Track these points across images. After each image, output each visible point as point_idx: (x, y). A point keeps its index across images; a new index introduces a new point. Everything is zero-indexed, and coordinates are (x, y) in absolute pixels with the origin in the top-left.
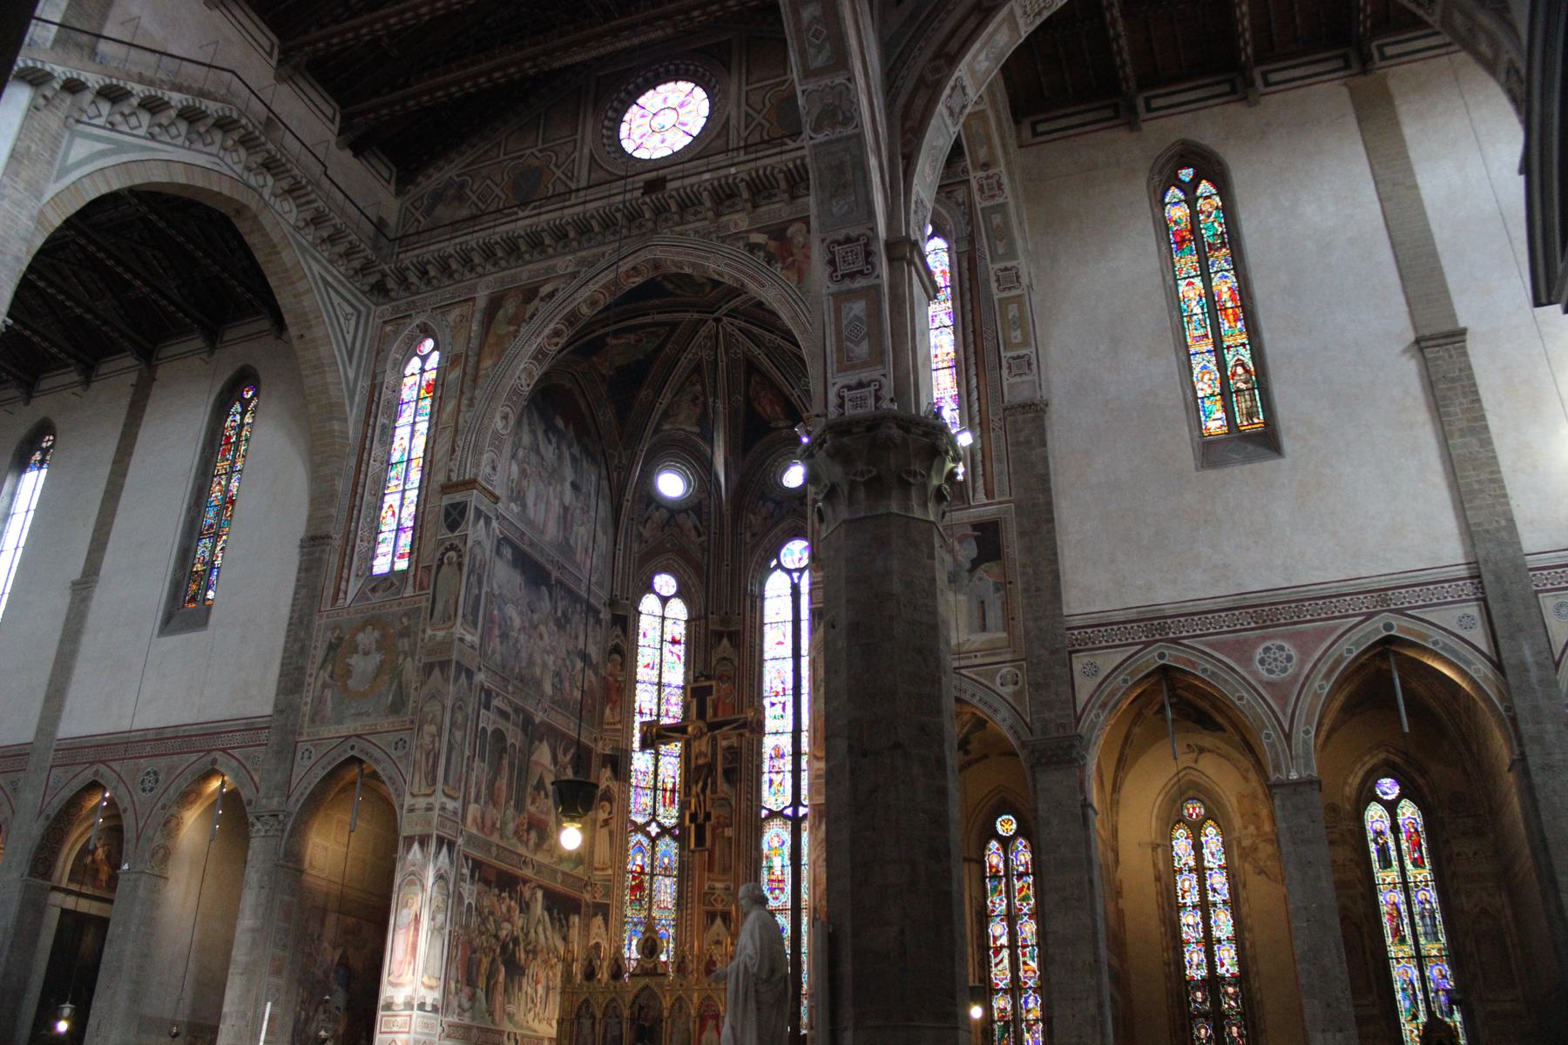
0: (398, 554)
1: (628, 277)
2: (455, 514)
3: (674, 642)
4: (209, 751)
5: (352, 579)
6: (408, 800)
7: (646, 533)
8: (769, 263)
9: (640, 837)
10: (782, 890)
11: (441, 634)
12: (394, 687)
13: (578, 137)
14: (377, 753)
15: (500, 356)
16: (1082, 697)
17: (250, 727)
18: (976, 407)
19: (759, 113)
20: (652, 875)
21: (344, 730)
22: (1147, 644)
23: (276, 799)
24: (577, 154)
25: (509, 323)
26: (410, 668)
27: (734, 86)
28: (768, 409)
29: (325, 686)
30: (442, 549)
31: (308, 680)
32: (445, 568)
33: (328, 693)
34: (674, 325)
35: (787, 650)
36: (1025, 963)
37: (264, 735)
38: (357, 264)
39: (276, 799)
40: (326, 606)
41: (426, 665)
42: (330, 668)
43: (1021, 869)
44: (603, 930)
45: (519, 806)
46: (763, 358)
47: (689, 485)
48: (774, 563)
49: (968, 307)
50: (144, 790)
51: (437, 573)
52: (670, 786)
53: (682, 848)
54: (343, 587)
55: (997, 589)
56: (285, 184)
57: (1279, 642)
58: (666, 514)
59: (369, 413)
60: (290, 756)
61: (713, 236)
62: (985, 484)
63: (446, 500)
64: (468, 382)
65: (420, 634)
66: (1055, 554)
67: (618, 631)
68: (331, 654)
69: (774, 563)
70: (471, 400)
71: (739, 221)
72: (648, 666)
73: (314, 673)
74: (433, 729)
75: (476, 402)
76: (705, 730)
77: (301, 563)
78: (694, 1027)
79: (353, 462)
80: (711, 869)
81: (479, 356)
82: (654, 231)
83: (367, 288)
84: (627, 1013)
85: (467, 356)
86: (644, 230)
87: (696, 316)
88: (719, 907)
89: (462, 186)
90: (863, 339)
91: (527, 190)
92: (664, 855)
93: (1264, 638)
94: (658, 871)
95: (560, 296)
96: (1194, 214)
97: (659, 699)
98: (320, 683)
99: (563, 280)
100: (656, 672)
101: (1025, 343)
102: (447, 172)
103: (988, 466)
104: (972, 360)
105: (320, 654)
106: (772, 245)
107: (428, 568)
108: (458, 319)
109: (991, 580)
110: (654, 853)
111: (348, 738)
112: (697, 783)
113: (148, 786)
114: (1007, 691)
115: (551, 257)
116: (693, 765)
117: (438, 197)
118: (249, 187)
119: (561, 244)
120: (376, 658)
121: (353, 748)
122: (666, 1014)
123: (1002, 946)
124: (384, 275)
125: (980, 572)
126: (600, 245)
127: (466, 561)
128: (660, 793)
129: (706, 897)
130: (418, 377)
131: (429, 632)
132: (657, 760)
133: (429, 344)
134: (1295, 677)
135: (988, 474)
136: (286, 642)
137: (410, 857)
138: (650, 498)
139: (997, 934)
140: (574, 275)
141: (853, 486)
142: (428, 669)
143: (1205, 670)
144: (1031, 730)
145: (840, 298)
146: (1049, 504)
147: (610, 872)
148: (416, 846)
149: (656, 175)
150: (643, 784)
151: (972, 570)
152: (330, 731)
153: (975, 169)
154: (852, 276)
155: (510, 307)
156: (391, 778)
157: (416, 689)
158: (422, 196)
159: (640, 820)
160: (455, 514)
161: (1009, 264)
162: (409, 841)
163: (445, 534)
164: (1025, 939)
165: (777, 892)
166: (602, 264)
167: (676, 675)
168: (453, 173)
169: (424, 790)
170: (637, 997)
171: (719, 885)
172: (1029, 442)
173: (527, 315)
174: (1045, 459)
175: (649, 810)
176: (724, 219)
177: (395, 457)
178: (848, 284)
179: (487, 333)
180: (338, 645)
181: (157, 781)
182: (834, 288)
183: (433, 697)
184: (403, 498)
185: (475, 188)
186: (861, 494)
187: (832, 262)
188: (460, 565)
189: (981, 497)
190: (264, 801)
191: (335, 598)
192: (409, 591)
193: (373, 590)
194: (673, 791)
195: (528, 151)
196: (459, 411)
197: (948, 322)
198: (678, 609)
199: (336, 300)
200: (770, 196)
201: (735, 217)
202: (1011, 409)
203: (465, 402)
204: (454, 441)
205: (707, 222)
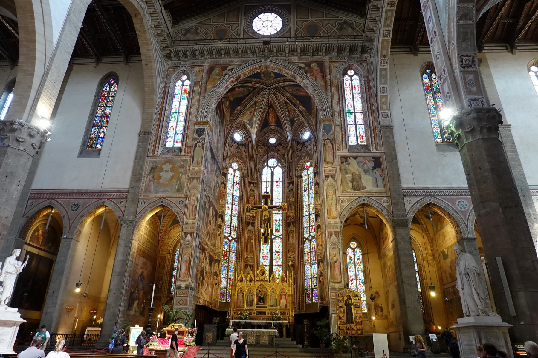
0: (175, 141)
1: (257, 69)
2: (201, 132)
3: (237, 183)
4: (101, 199)
5: (160, 147)
6: (185, 220)
7: (232, 150)
8: (306, 73)
9: (226, 240)
10: (267, 259)
11: (196, 168)
12: (178, 183)
13: (239, 22)
14: (172, 204)
15: (214, 85)
16: (407, 209)
17: (119, 192)
18: (372, 125)
19: (301, 28)
20: (229, 252)
21: (158, 196)
22: (426, 197)
23: (131, 217)
24: (239, 28)
25: (217, 75)
26: (184, 178)
27: (292, 18)
28: (271, 119)
29: (150, 181)
30: (196, 142)
31: (143, 178)
32: (197, 148)
33: (152, 183)
34: (255, 88)
36: (360, 284)
37: (125, 195)
38: (164, 45)
39: (131, 217)
40: (150, 154)
41: (191, 178)
42: (152, 175)
43: (358, 257)
44: (218, 268)
45: (207, 228)
46: (277, 104)
47: (243, 138)
48: (266, 164)
49: (368, 96)
50: (72, 210)
51: (194, 149)
52: (235, 226)
53: (238, 244)
54: (157, 149)
55: (381, 176)
56: (152, 11)
57: (463, 200)
58: (237, 145)
59: (164, 95)
60: (137, 203)
61: (287, 62)
62: (375, 146)
63: (197, 127)
64: (203, 91)
65: (188, 168)
66: (398, 169)
67: (224, 177)
68: (153, 170)
69: (266, 164)
70: (204, 97)
71: (296, 59)
72: (229, 189)
73: (146, 176)
74: (195, 198)
75: (206, 98)
76: (267, 208)
77: (139, 140)
78: (278, 298)
79: (159, 110)
80: (247, 252)
81: (206, 83)
82: (267, 57)
83: (165, 55)
84: (255, 293)
85: (202, 83)
86: (263, 56)
87: (264, 87)
88: (249, 263)
89: (197, 29)
90: (474, 86)
91: (221, 35)
92: (233, 246)
93: (459, 199)
94: (231, 251)
95: (235, 70)
96: (431, 82)
97: (233, 199)
98: (148, 179)
99: (236, 66)
100: (232, 191)
101: (387, 109)
103: (376, 141)
104: (370, 111)
105: (148, 171)
106: (307, 68)
107: (190, 147)
108: (198, 71)
109: (379, 173)
110: (230, 246)
111: (160, 198)
112: (264, 224)
113: (74, 209)
114: (385, 205)
115: (231, 58)
116: (263, 219)
117: (188, 31)
118: (141, 7)
119: (235, 54)
120: (171, 174)
121: (162, 202)
122: (268, 293)
123: (353, 279)
124: (171, 51)
125: (375, 170)
126: (248, 57)
127: (205, 147)
128: (232, 227)
129: (246, 259)
130: (181, 87)
131: (192, 167)
132: (232, 218)
134: (468, 210)
135: (376, 143)
136: (134, 165)
137: (187, 238)
138: (233, 140)
139: (352, 275)
140: (240, 65)
141: (482, 128)
142: (193, 179)
143: (442, 205)
144: (393, 216)
145: (464, 74)
146: (396, 155)
147: (220, 250)
148: (189, 235)
149: (267, 41)
150: (228, 224)
151: (373, 170)
152: (153, 196)
153: (381, 56)
154: (468, 67)
155: (217, 70)
156: (177, 213)
157: (187, 185)
158: (182, 30)
159: (227, 235)
160: (201, 132)
161: (385, 86)
162: (186, 234)
163: (196, 137)
164: (360, 277)
165: (265, 260)
166: (249, 63)
167: (237, 193)
168: (193, 24)
169: (191, 218)
170: (258, 287)
171: (249, 257)
172: (388, 137)
173: (224, 73)
174: (394, 142)
175: (229, 232)
176: (291, 57)
178: (466, 69)
179: (209, 77)
180: (156, 168)
181: (78, 207)
182: (463, 69)
183: (194, 188)
184: (177, 124)
185: (202, 31)
186: (485, 131)
187: (462, 62)
188: (203, 148)
189: (374, 150)
190: (126, 217)
191: (154, 153)
192: (183, 153)
193: (167, 152)
194: (235, 227)
195: (221, 23)
196: (200, 100)
197: (360, 100)
198: (238, 174)
199: (158, 55)
200: (305, 54)
201: (294, 57)
202: (383, 127)
203: (202, 97)
204: (198, 109)
205: (285, 57)
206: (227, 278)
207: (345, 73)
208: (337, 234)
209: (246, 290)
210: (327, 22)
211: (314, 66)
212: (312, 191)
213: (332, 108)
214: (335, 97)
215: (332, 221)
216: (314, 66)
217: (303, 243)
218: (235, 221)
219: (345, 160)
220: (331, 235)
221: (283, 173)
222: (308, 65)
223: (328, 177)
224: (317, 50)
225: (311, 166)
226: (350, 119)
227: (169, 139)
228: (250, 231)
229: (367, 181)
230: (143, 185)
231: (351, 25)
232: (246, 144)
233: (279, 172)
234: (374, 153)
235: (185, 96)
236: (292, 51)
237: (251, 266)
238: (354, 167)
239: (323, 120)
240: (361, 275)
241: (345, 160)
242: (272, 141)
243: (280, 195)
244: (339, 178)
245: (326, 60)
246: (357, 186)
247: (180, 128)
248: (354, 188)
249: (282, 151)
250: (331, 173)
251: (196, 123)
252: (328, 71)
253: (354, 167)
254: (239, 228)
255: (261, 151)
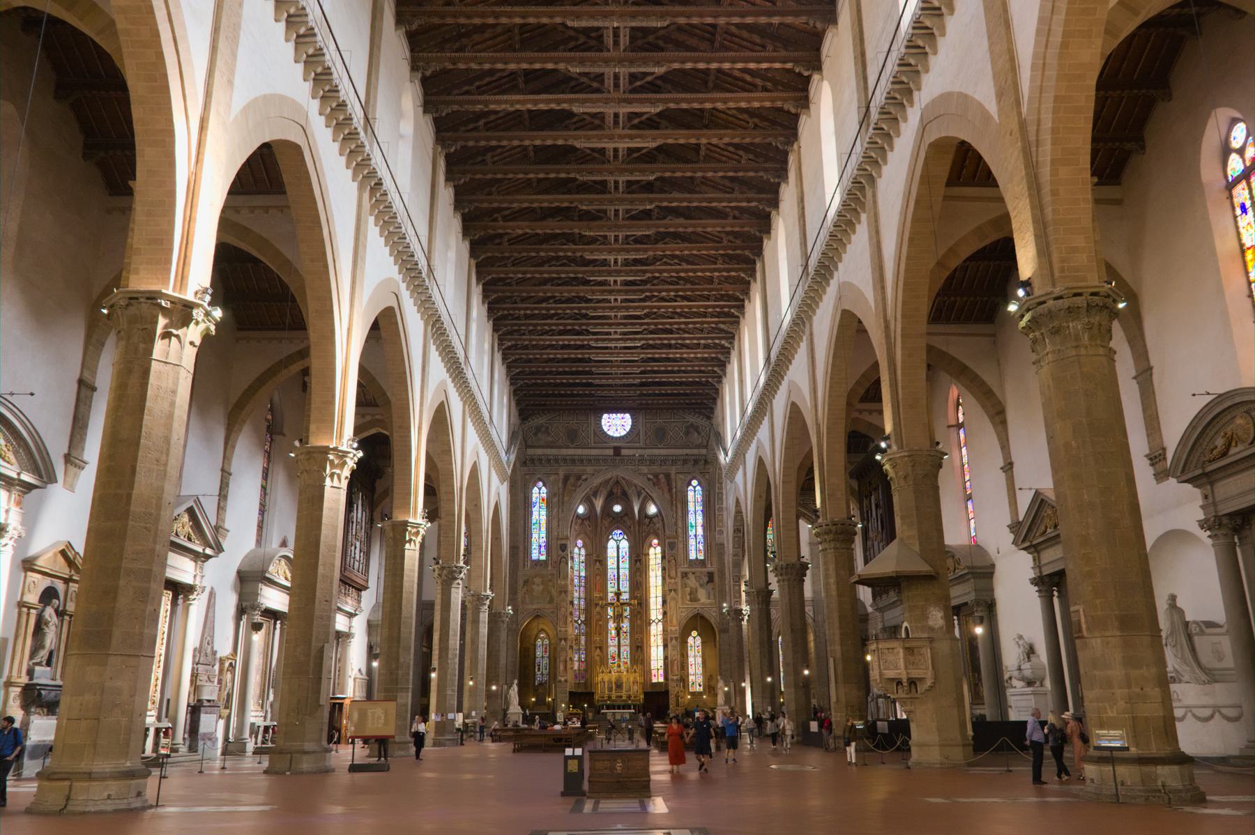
21: (534, 607)
26: (554, 592)
27: (641, 418)
35: (615, 566)
40: (521, 568)
63: (559, 542)
71: (645, 469)
79: (522, 522)
89: (547, 428)
91: (573, 437)
102: (540, 420)
117: (538, 429)
120: (541, 587)
133: (541, 484)
152: (530, 607)
155: (572, 480)
162: (561, 640)
163: (560, 552)
167: (583, 574)
177: (534, 521)
198: (583, 552)
202: (717, 545)
206: (579, 660)
207: (690, 484)
208: (676, 638)
209: (606, 679)
210: (674, 424)
211: (661, 476)
212: (659, 573)
213: (676, 524)
214: (680, 513)
215: (673, 629)
216: (661, 476)
217: (650, 624)
218: (582, 603)
219: (685, 575)
220: (672, 639)
221: (630, 548)
222: (656, 476)
223: (670, 590)
224: (664, 461)
225: (659, 544)
226: (692, 533)
227: (534, 551)
228: (599, 613)
229: (702, 595)
230: (520, 596)
231: (697, 429)
232: (590, 516)
233: (625, 545)
234: (709, 568)
235: (544, 505)
236: (642, 460)
237: (601, 648)
238: (692, 582)
239: (669, 538)
240: (700, 660)
241: (685, 575)
242: (617, 508)
243: (627, 572)
244: (680, 592)
245: (673, 472)
246: (694, 599)
247: (543, 541)
248: (691, 600)
249: (629, 523)
250: (674, 587)
251: (558, 539)
252: (674, 484)
253: (692, 582)
254: (587, 610)
255: (606, 523)
